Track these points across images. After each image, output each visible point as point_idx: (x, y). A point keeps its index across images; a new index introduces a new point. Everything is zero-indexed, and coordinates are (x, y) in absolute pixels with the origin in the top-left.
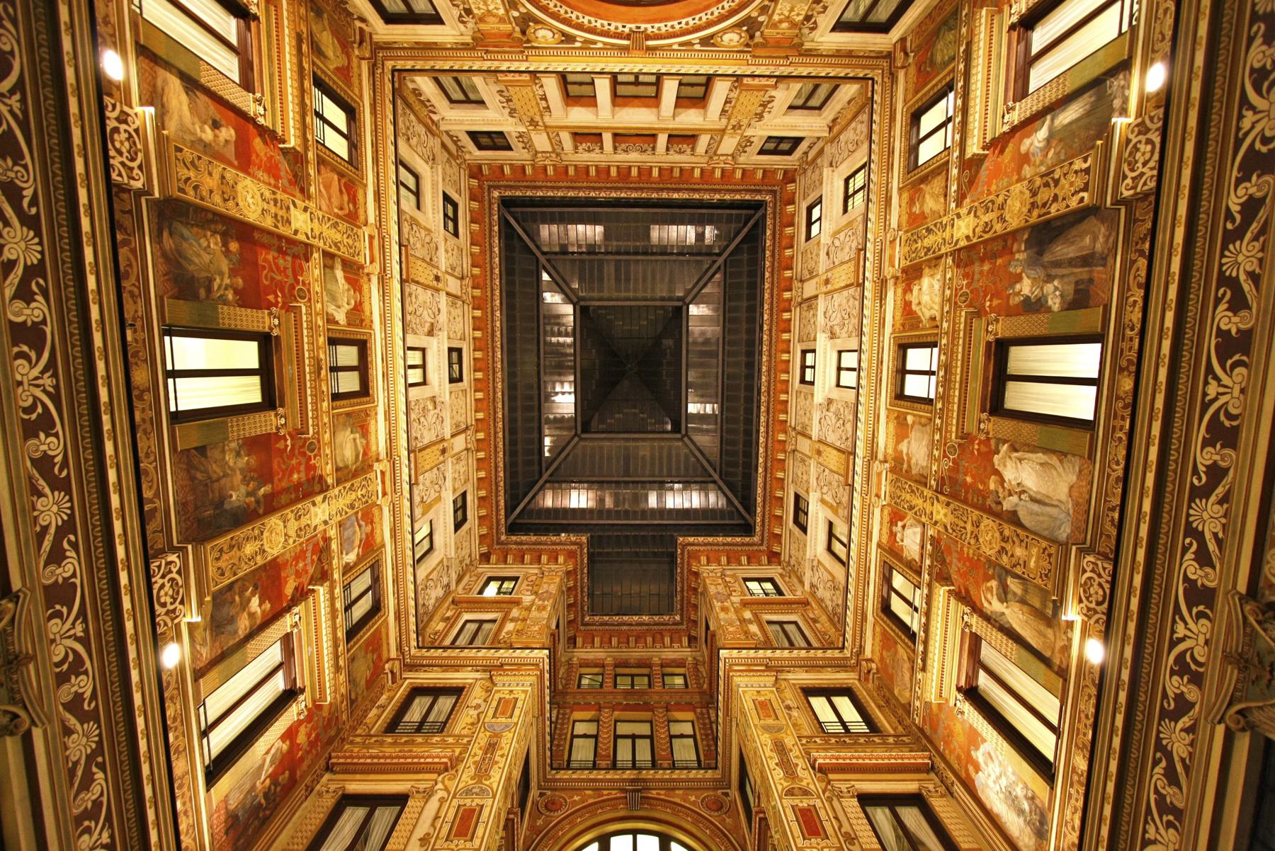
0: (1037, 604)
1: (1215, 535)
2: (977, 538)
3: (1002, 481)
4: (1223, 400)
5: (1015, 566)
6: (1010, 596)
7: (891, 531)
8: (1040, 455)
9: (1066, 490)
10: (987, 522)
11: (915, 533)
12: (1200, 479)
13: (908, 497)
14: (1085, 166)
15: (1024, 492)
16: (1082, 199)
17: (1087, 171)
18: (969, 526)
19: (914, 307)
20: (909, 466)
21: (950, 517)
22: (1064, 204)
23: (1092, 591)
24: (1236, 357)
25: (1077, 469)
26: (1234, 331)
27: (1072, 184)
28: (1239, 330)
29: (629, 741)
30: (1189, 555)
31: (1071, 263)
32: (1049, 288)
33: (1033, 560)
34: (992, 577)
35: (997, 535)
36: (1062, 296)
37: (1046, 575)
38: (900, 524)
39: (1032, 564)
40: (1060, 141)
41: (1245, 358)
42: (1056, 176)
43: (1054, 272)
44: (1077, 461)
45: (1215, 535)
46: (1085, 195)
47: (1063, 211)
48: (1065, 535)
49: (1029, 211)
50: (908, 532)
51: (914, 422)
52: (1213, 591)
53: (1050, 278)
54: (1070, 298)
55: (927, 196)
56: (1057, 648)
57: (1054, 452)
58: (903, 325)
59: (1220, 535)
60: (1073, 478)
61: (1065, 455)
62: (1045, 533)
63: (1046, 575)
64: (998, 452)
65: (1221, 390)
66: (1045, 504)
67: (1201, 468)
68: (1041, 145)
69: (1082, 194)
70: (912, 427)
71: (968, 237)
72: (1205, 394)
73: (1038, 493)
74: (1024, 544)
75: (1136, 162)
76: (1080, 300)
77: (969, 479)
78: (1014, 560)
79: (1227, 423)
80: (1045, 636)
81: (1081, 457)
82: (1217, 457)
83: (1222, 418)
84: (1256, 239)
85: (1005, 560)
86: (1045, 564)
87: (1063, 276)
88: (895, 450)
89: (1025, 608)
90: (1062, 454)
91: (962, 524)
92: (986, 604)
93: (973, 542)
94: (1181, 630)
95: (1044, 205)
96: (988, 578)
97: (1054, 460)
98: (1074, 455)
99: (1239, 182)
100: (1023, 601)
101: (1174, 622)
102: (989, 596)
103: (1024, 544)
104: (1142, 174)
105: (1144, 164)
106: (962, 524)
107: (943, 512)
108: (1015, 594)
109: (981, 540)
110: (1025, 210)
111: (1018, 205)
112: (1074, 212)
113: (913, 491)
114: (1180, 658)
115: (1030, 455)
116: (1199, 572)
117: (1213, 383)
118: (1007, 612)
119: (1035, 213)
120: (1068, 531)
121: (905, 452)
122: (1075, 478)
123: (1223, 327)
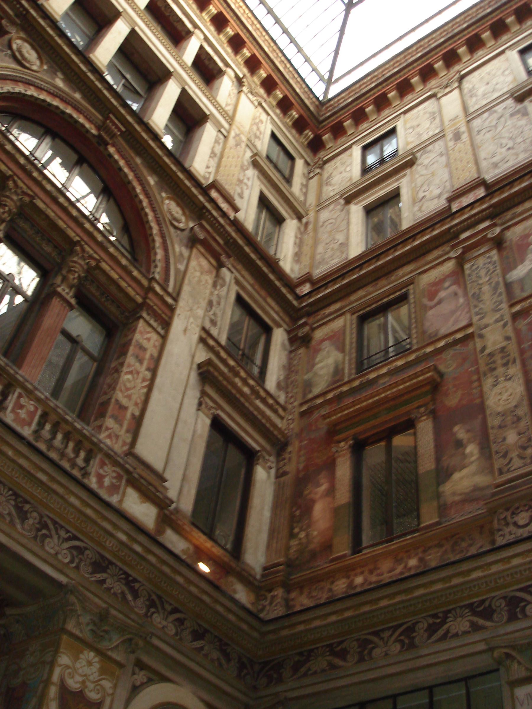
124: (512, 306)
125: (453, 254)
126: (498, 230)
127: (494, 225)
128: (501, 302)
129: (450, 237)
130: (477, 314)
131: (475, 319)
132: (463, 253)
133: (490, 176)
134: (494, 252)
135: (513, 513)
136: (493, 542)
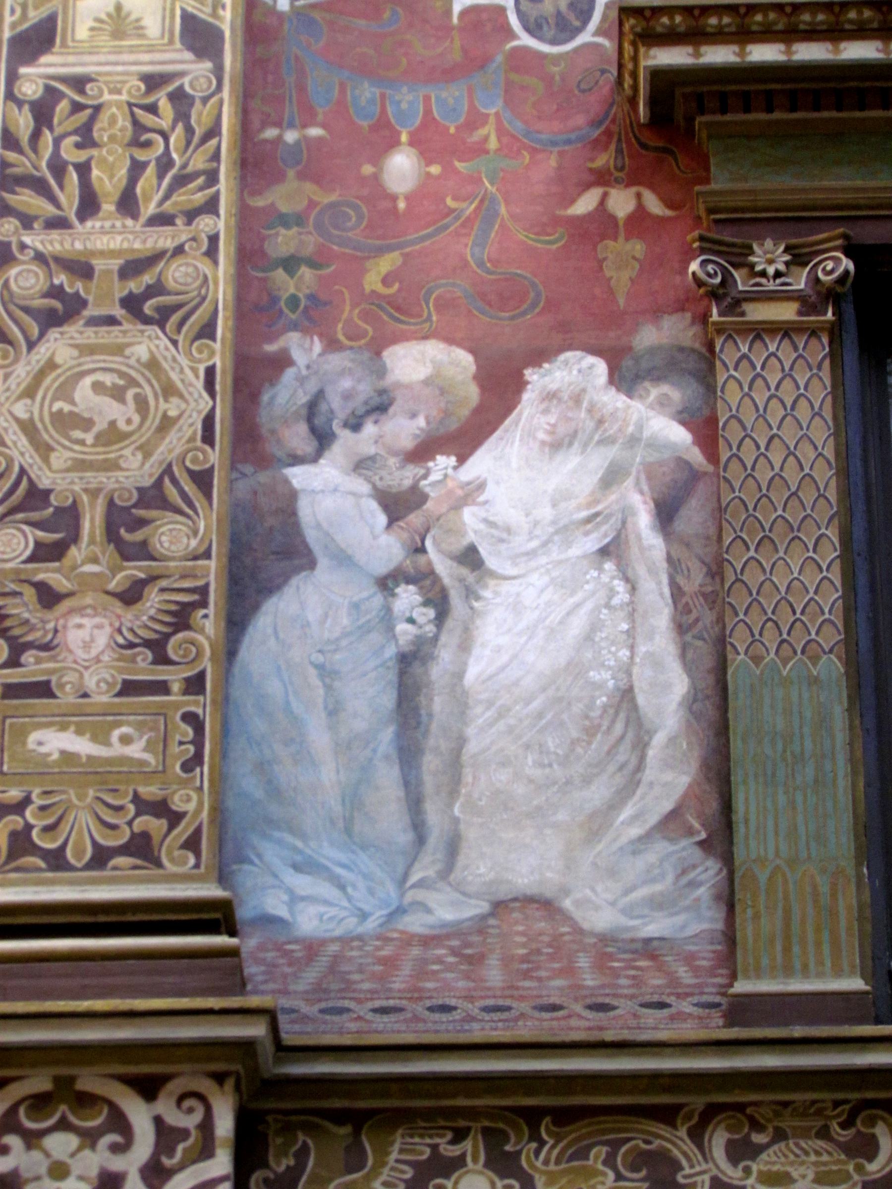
2: (61, 310)
3: (465, 437)
10: (190, 372)
15: (439, 602)
18: (108, 238)
21: (115, 75)
23: (61, 1144)
25: (654, 927)
35: (135, 471)
37: (20, 843)
39: (53, 742)
44: (689, 922)
48: (275, 904)
57: (719, 773)
61: (721, 836)
62: (246, 782)
64: (625, 375)
66: (408, 754)
74: (144, 668)
77: (402, 168)
86: (82, 830)
90: (717, 820)
91: (108, 181)
97: (671, 777)
98: (728, 900)
103: (144, 668)
109: (59, 345)
115: (662, 618)
120: (308, 922)
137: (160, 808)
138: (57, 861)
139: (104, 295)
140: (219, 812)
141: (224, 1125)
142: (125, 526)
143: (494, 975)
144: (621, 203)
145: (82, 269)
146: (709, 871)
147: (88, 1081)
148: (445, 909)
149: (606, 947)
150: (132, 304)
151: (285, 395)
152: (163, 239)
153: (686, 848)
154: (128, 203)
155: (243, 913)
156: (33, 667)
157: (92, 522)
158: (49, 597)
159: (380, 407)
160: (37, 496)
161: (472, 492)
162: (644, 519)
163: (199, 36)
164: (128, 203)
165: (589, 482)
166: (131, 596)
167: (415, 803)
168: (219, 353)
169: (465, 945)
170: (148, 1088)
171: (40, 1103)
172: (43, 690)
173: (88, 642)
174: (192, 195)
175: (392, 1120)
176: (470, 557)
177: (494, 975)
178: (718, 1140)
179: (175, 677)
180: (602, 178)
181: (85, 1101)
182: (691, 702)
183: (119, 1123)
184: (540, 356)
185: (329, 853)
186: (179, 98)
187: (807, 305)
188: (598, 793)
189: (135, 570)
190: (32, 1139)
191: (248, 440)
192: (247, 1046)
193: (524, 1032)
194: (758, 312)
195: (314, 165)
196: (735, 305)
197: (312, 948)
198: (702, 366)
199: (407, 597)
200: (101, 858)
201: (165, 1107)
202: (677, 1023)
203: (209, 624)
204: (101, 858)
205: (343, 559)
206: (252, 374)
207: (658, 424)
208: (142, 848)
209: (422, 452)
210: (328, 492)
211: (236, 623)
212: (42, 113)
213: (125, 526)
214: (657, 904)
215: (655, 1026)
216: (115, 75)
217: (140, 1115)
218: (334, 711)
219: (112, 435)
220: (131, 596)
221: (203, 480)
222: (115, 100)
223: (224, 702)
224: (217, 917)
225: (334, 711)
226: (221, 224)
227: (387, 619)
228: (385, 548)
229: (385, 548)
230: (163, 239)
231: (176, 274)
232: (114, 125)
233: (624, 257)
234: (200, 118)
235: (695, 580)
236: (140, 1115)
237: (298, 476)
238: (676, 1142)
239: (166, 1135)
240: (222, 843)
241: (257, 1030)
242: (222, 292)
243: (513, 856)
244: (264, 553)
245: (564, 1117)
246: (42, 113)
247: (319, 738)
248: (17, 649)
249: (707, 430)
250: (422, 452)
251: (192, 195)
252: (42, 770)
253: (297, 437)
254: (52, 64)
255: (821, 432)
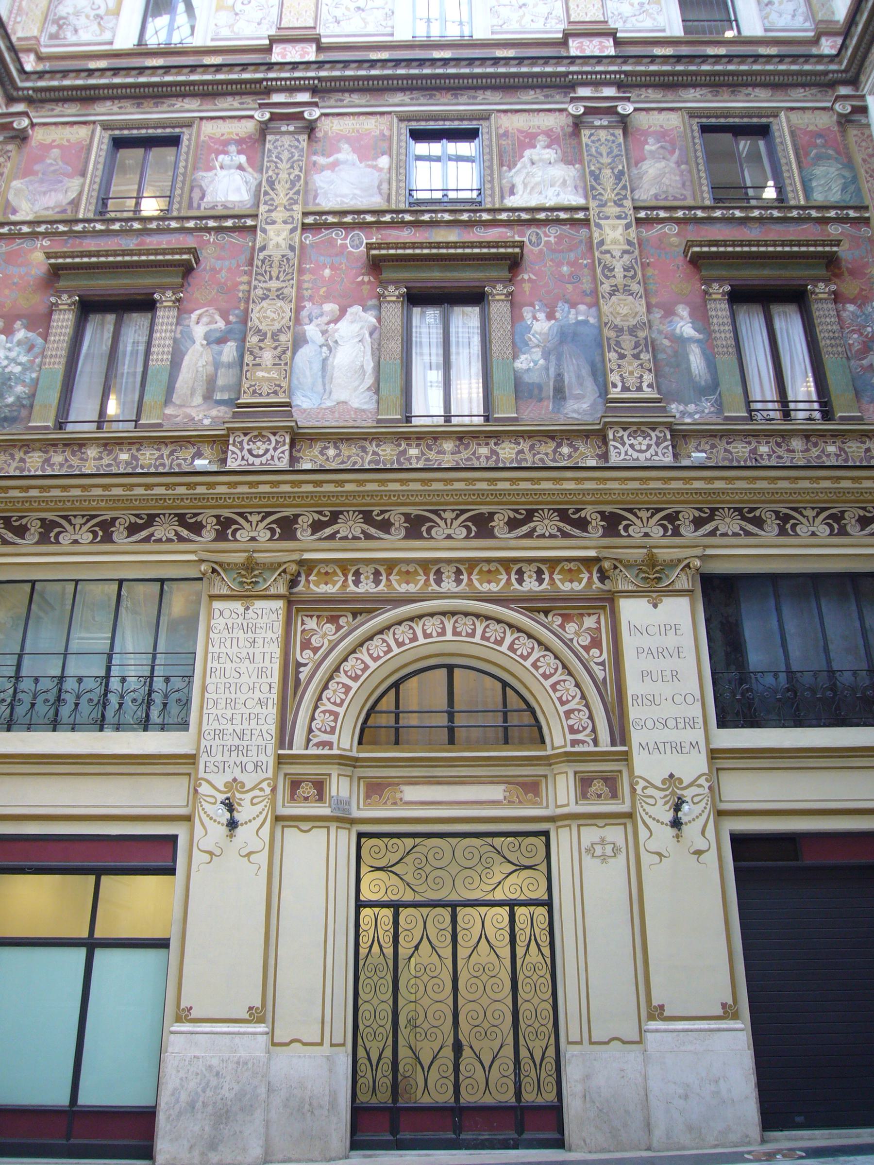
0: (220, 382)
1: (338, 532)
2: (265, 298)
3: (336, 321)
4: (441, 523)
5: (251, 353)
6: (215, 347)
7: (226, 143)
8: (372, 364)
9: (342, 399)
10: (287, 309)
11: (238, 190)
12: (378, 515)
13: (283, 176)
14: (645, 388)
16: (615, 386)
17: (639, 389)
18: (274, 284)
19: (527, 153)
20: (323, 168)
21: (277, 255)
22: (615, 367)
23: (259, 444)
24: (474, 528)
25: (365, 407)
26: (492, 524)
27: (631, 373)
28: (493, 527)
29: (446, 913)
30: (316, 517)
31: (559, 377)
32: (537, 354)
33: (266, 375)
34: (228, 322)
35: (277, 326)
36: (528, 370)
37: (254, 392)
38: (243, 159)
39: (260, 374)
40: (676, 352)
41: (473, 534)
42: (642, 356)
43: (553, 358)
44: (371, 406)
45: (338, 532)
46: (619, 389)
47: (608, 365)
49: (616, 326)
50: (237, 175)
51: (380, 170)
52: (294, 538)
53: (546, 355)
54: (527, 379)
55: (663, 164)
56: (188, 410)
57: (378, 380)
58: (506, 134)
59: (338, 536)
60: (356, 405)
61: (377, 392)
62: (295, 382)
63: (254, 392)
64: (365, 310)
65: (449, 522)
66: (323, 377)
67: (386, 516)
68: (678, 331)
69: (620, 385)
70: (375, 167)
71: (602, 243)
72: (444, 511)
73: (333, 368)
74: (277, 361)
75: (635, 438)
76: (522, 390)
77: (327, 272)
78: (256, 351)
79: (424, 529)
80: (192, 394)
81: (378, 411)
82: (397, 525)
83: (428, 525)
84: (559, 530)
85: (253, 340)
86: (265, 389)
87: (547, 369)
88: (340, 137)
89: (210, 369)
90: (377, 388)
91: (274, 274)
92: (194, 316)
93: (259, 292)
94: (254, 518)
95: (618, 344)
96: (224, 315)
97: (369, 381)
98: (378, 402)
99: (602, 513)
100: (217, 365)
101: (259, 513)
102: (205, 320)
103: (277, 361)
104: (623, 444)
105: (632, 446)
106: (274, 274)
107: (280, 240)
108: (220, 353)
109: (265, 304)
110: (618, 321)
111: (624, 311)
112: (605, 375)
113: (293, 184)
114: (232, 522)
116: (305, 525)
117: (454, 515)
118: (197, 347)
119: (612, 334)
120: (304, 406)
121: (340, 156)
122: (356, 405)
123: (496, 517)
124: (305, 214)
125: (257, 115)
126: (316, 113)
127: (316, 104)
128: (296, 202)
129: (259, 90)
130: (265, 203)
131: (263, 208)
132: (270, 120)
133: (330, 33)
134: (306, 137)
135: (250, 440)
136: (224, 461)
137: (279, 386)
138: (261, 395)
139: (273, 295)
140: (289, 386)
141: (288, 440)
142: (275, 336)
143: (337, 415)
144: (366, 279)
145: (269, 290)
146: (375, 397)
147: (264, 433)
148: (329, 404)
149: (356, 410)
150: (278, 296)
151: (304, 313)
152: (284, 285)
153: (371, 393)
154: (278, 278)
155: (293, 404)
156: (258, 361)
157: (269, 335)
158: (261, 348)
159: (321, 315)
160: (260, 331)
161: (336, 331)
162: (367, 335)
163: (292, 248)
164: (278, 278)
165: (357, 329)
166: (275, 348)
167: (324, 385)
168: (293, 305)
169: (331, 410)
170: (274, 434)
171: (256, 437)
172: (259, 365)
173: (268, 356)
174: (289, 277)
175: (319, 439)
176: (336, 342)
177: (337, 415)
178: (374, 444)
179: (282, 363)
180: (363, 274)
181: (264, 436)
182: (374, 368)
183: (269, 440)
184: (350, 306)
185: (309, 394)
186: (288, 259)
187: (398, 297)
188: (357, 383)
189: (276, 344)
190: (254, 443)
191: (297, 321)
192: (292, 427)
193: (341, 424)
194: (388, 299)
195: (312, 271)
196: (385, 297)
197: (305, 410)
198: (379, 308)
199: (325, 349)
200: (268, 394)
201: (277, 437)
202: (367, 423)
203: (289, 353)
204: (268, 394)
205: (313, 342)
206: (298, 309)
207: (370, 318)
208: (275, 392)
209: (328, 323)
210: (312, 330)
211: (294, 353)
212: (263, 262)
213: (275, 336)
214: (366, 403)
215: (364, 424)
216: (277, 255)
217: (273, 438)
218: (311, 369)
219: (273, 320)
220: (275, 348)
221: (289, 328)
222: (276, 260)
223: (291, 367)
224: (288, 405)
225: (311, 369)
226: (294, 282)
227: (321, 353)
228: (320, 340)
229: (320, 340)
230: (284, 285)
231: (286, 291)
232: (276, 264)
233: (366, 289)
234: (291, 263)
235: (376, 346)
236: (273, 438)
237: (306, 327)
238: (366, 444)
239: (277, 442)
240: (290, 392)
241: (293, 424)
242: (294, 294)
243: (341, 394)
244: (299, 341)
245: (348, 439)
246: (263, 262)
247: (308, 373)
248: (255, 358)
249: (379, 320)
250: (328, 323)
251: (289, 277)
252: (258, 379)
253: (306, 320)
254: (265, 253)
255: (399, 320)
